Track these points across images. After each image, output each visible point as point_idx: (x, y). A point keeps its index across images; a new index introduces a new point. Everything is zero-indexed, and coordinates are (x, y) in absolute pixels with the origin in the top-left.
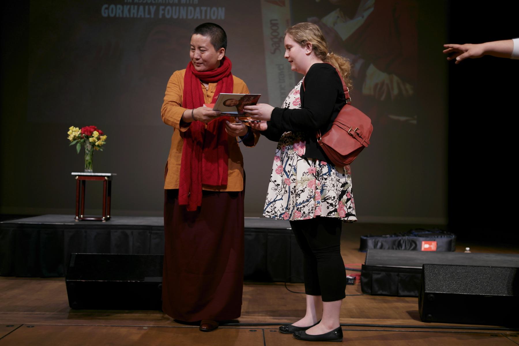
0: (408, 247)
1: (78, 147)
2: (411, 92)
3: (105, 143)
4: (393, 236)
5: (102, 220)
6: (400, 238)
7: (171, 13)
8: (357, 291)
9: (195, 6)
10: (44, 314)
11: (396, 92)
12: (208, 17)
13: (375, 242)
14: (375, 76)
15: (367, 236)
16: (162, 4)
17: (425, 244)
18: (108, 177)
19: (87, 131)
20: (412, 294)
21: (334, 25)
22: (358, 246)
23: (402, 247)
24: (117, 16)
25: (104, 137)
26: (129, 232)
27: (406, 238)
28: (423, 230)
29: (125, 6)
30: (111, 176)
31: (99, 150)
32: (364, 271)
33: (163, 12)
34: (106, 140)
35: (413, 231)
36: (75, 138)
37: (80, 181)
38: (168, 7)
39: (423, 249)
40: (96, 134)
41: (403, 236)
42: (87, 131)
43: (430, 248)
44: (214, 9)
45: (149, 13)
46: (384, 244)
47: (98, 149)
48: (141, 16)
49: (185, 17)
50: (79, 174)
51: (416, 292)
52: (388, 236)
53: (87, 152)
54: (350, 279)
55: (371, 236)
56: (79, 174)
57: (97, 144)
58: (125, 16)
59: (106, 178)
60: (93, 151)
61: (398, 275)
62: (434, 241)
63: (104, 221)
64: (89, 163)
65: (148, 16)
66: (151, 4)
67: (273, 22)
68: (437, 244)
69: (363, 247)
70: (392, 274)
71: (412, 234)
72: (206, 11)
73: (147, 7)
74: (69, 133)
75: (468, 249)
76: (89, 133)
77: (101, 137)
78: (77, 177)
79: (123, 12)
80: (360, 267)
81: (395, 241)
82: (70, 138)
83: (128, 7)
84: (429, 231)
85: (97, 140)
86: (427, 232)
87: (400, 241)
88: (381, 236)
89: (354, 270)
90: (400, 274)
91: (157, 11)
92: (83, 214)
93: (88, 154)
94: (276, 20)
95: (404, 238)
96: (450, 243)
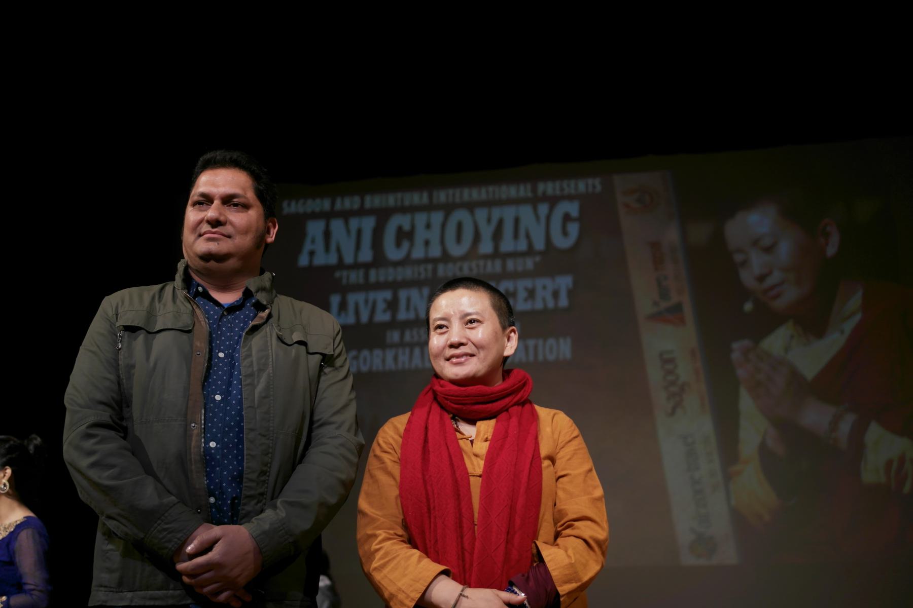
12: (540, 358)
14: (882, 447)
24: (374, 368)
44: (551, 341)
72: (536, 347)
79: (384, 361)
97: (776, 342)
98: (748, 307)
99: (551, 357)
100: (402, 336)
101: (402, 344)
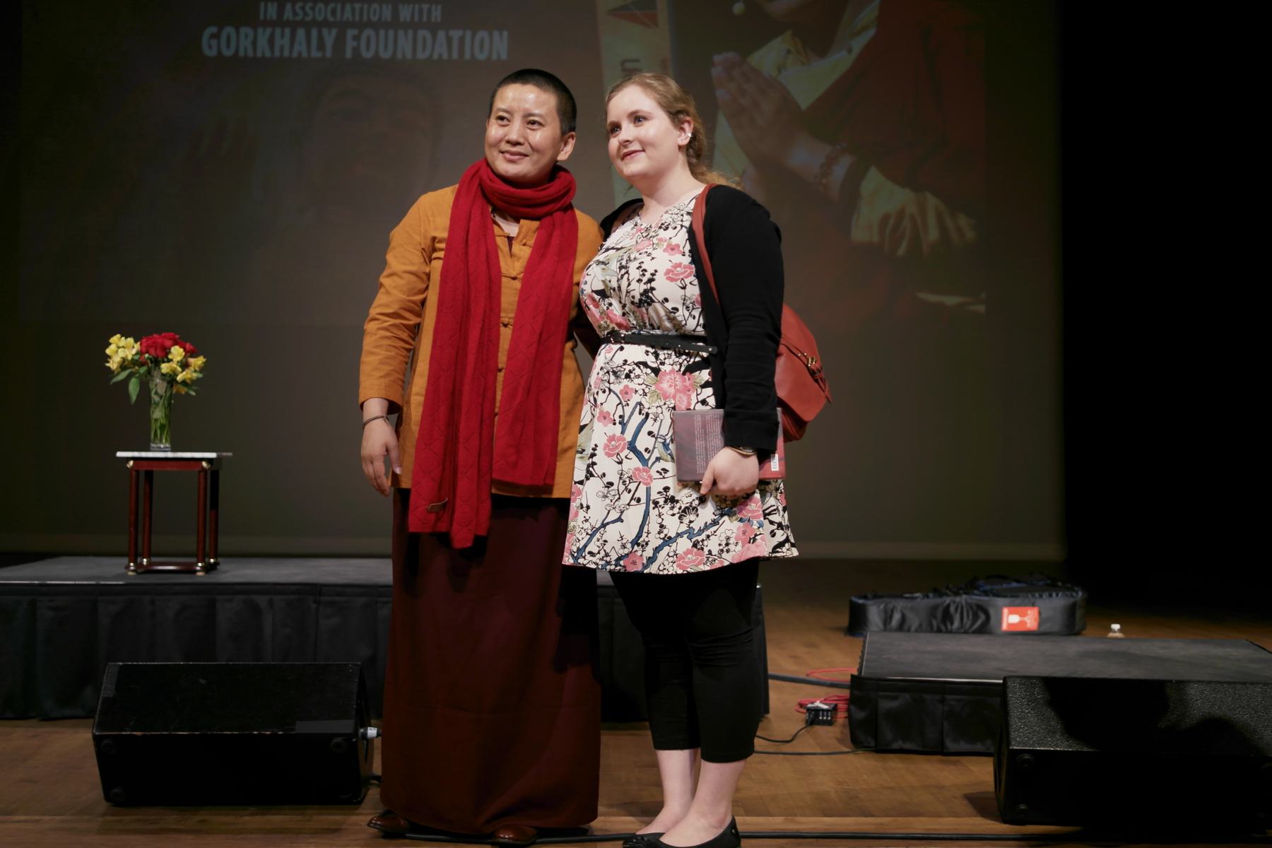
0: (967, 622)
1: (133, 388)
2: (970, 235)
3: (200, 376)
4: (931, 595)
5: (196, 571)
6: (948, 600)
7: (375, 46)
8: (840, 741)
9: (433, 28)
10: (37, 821)
11: (933, 234)
12: (467, 56)
13: (885, 611)
14: (882, 199)
15: (865, 597)
16: (352, 24)
17: (1011, 613)
18: (209, 460)
19: (154, 345)
20: (979, 747)
21: (779, 71)
22: (844, 620)
23: (952, 624)
25: (198, 361)
26: (262, 600)
27: (963, 599)
28: (1004, 578)
29: (260, 30)
30: (218, 459)
31: (187, 393)
32: (856, 692)
33: (355, 44)
34: (202, 369)
35: (981, 582)
36: (124, 365)
37: (137, 472)
38: (369, 32)
39: (1005, 627)
40: (177, 353)
41: (957, 594)
42: (154, 345)
43: (1022, 623)
44: (482, 34)
45: (321, 47)
46: (909, 615)
47: (183, 390)
48: (300, 53)
49: (409, 56)
50: (136, 454)
51: (989, 742)
52: (917, 595)
53: (156, 398)
54: (823, 710)
55: (876, 597)
56: (136, 454)
57: (179, 378)
58: (259, 54)
59: (204, 464)
60: (171, 397)
61: (942, 701)
62: (1033, 605)
63: (200, 574)
64: (162, 427)
65: (319, 55)
66: (326, 23)
67: (629, 65)
68: (1040, 613)
69: (856, 625)
70: (928, 697)
71: (977, 588)
72: (462, 40)
73: (314, 32)
74: (108, 351)
75: (1116, 627)
76: (160, 353)
77: (191, 360)
78: (131, 463)
79: (254, 43)
80: (849, 678)
81: (935, 608)
82: (113, 364)
83: (269, 31)
84: (1018, 581)
85: (179, 369)
86: (1014, 585)
87: (948, 606)
88: (901, 596)
89: (832, 685)
90: (948, 697)
91: (340, 41)
92: (148, 557)
93: (157, 404)
94: (637, 61)
95: (958, 599)
96: (1071, 611)
97: (768, 57)
98: (738, 8)
99: (481, 57)
100: (281, 11)
101: (280, 23)
